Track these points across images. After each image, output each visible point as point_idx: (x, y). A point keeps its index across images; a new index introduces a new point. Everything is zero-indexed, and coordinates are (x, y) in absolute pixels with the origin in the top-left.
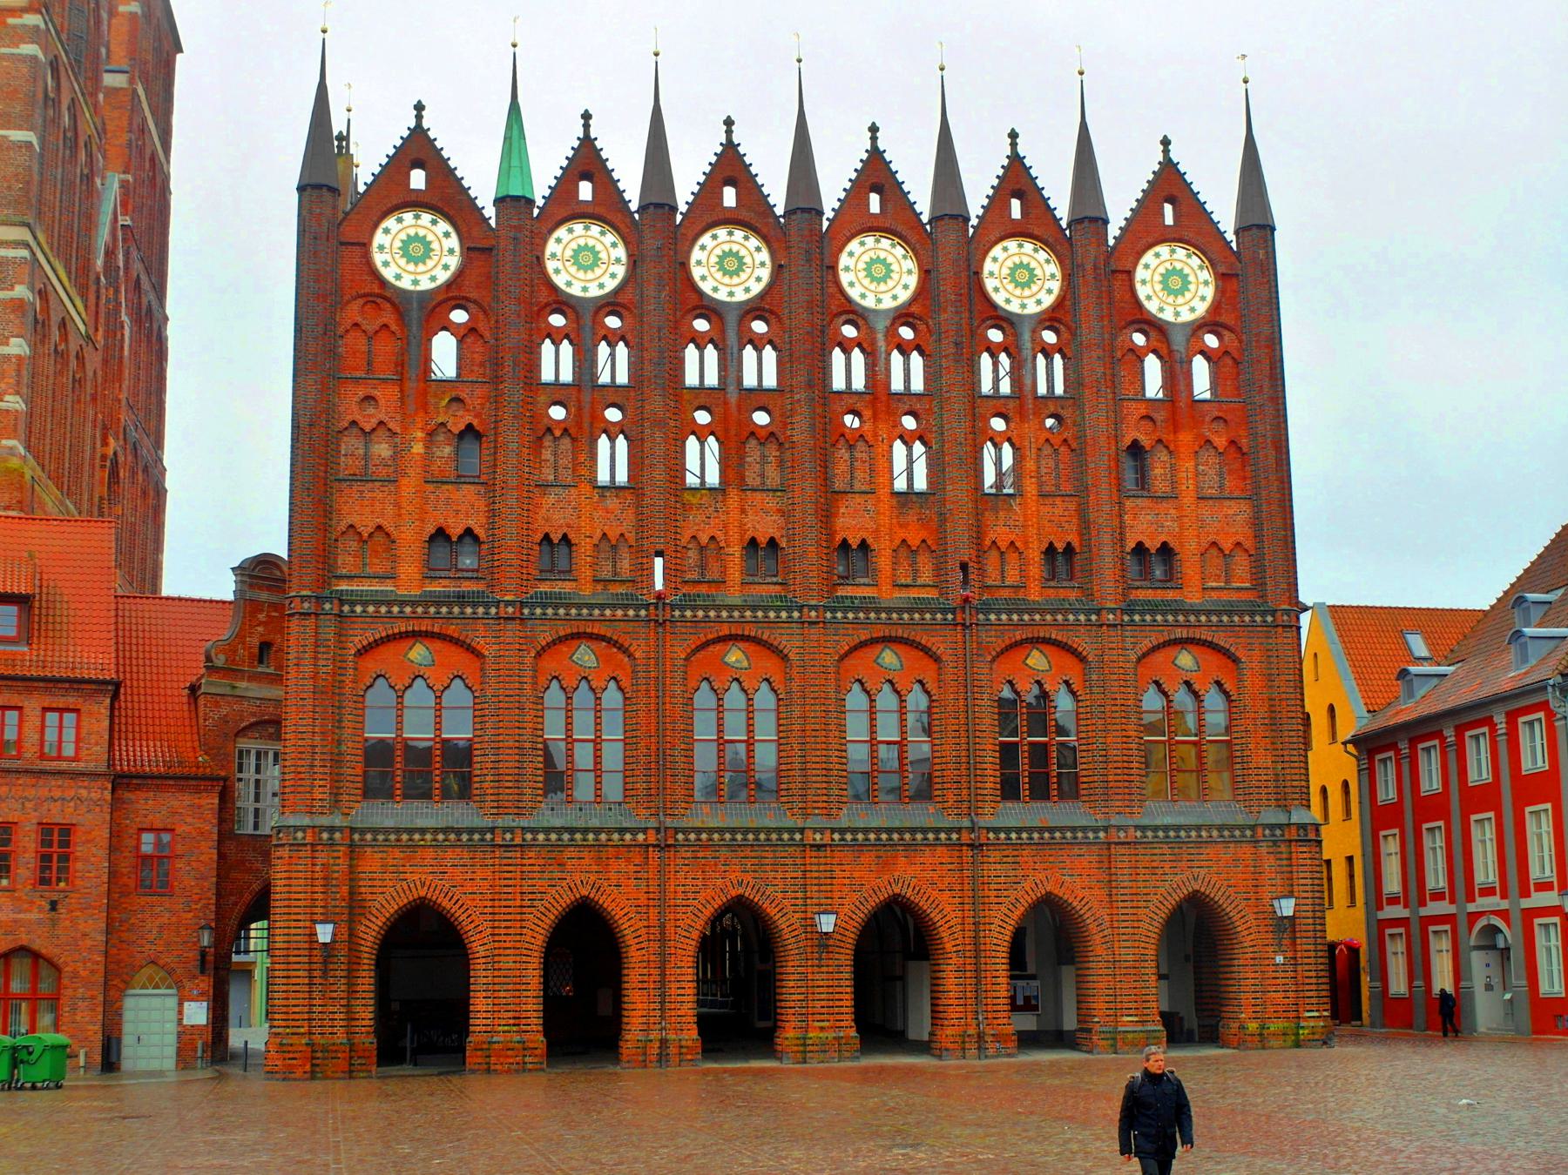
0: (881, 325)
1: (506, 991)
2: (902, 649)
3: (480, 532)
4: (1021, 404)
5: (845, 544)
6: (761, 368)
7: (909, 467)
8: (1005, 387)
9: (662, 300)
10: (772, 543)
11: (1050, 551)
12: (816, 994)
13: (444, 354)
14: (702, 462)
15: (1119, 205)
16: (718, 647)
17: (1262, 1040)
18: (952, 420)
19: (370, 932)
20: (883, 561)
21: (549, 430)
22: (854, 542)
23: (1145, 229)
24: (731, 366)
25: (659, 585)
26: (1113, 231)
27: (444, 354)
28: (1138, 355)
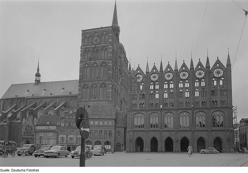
1: (147, 144)
2: (186, 113)
6: (172, 86)
7: (187, 95)
8: (198, 86)
9: (162, 80)
12: (177, 146)
13: (141, 87)
15: (211, 65)
17: (226, 152)
19: (135, 139)
20: (184, 104)
23: (215, 67)
24: (169, 86)
25: (161, 107)
26: (211, 68)
27: (141, 87)
28: (213, 81)
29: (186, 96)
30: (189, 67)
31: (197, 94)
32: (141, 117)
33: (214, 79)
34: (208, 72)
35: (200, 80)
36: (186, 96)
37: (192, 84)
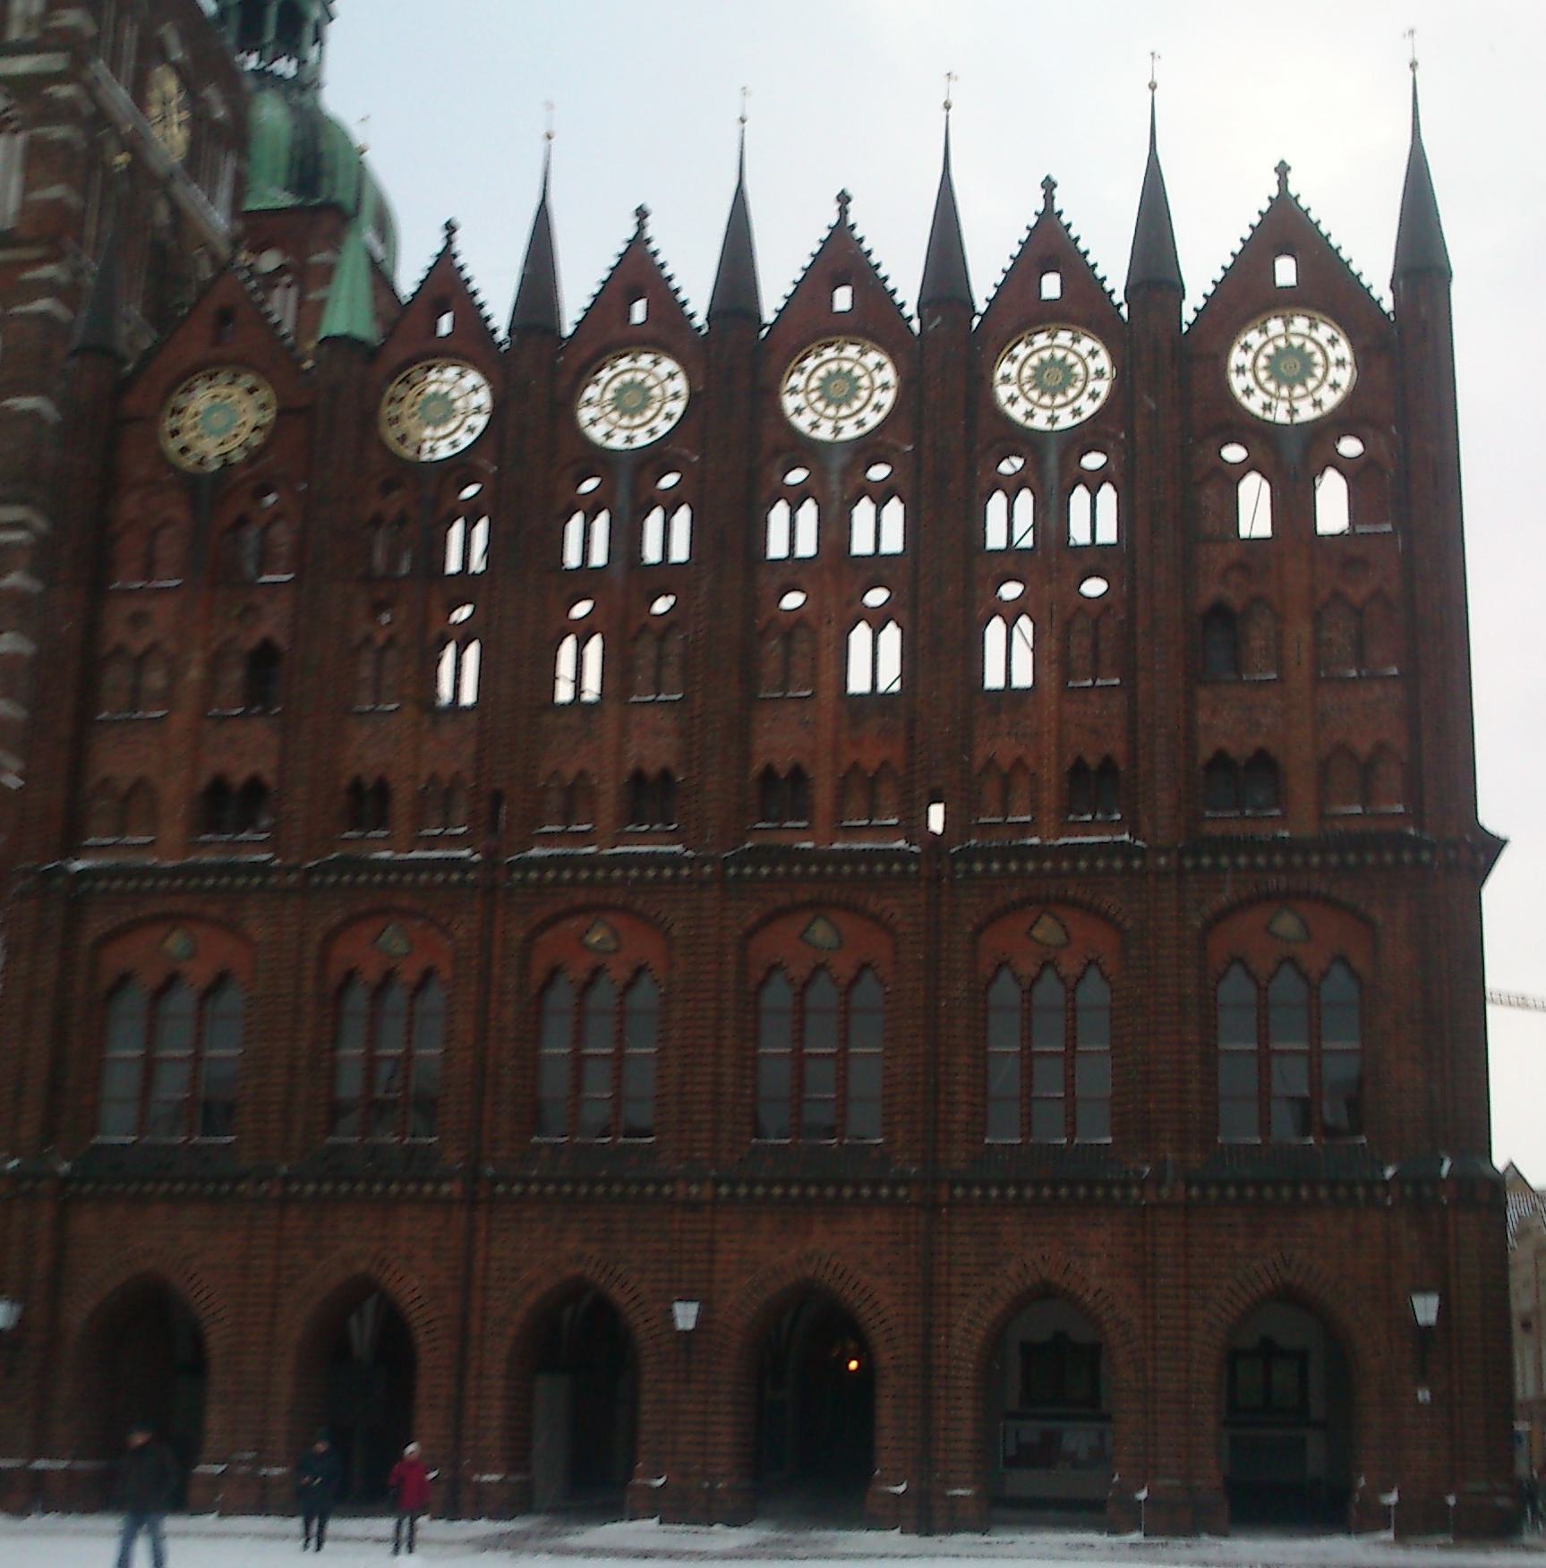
0: (837, 462)
3: (269, 778)
4: (1052, 556)
5: (769, 774)
6: (669, 537)
7: (874, 660)
10: (666, 776)
11: (1078, 769)
14: (579, 670)
16: (574, 923)
18: (942, 591)
20: (823, 794)
21: (368, 640)
22: (782, 769)
28: (1236, 474)
29: (858, 682)
30: (905, 279)
31: (1008, 656)
32: (199, 973)
33: (1234, 453)
34: (1167, 354)
35: (1052, 466)
36: (858, 682)
37: (944, 515)
